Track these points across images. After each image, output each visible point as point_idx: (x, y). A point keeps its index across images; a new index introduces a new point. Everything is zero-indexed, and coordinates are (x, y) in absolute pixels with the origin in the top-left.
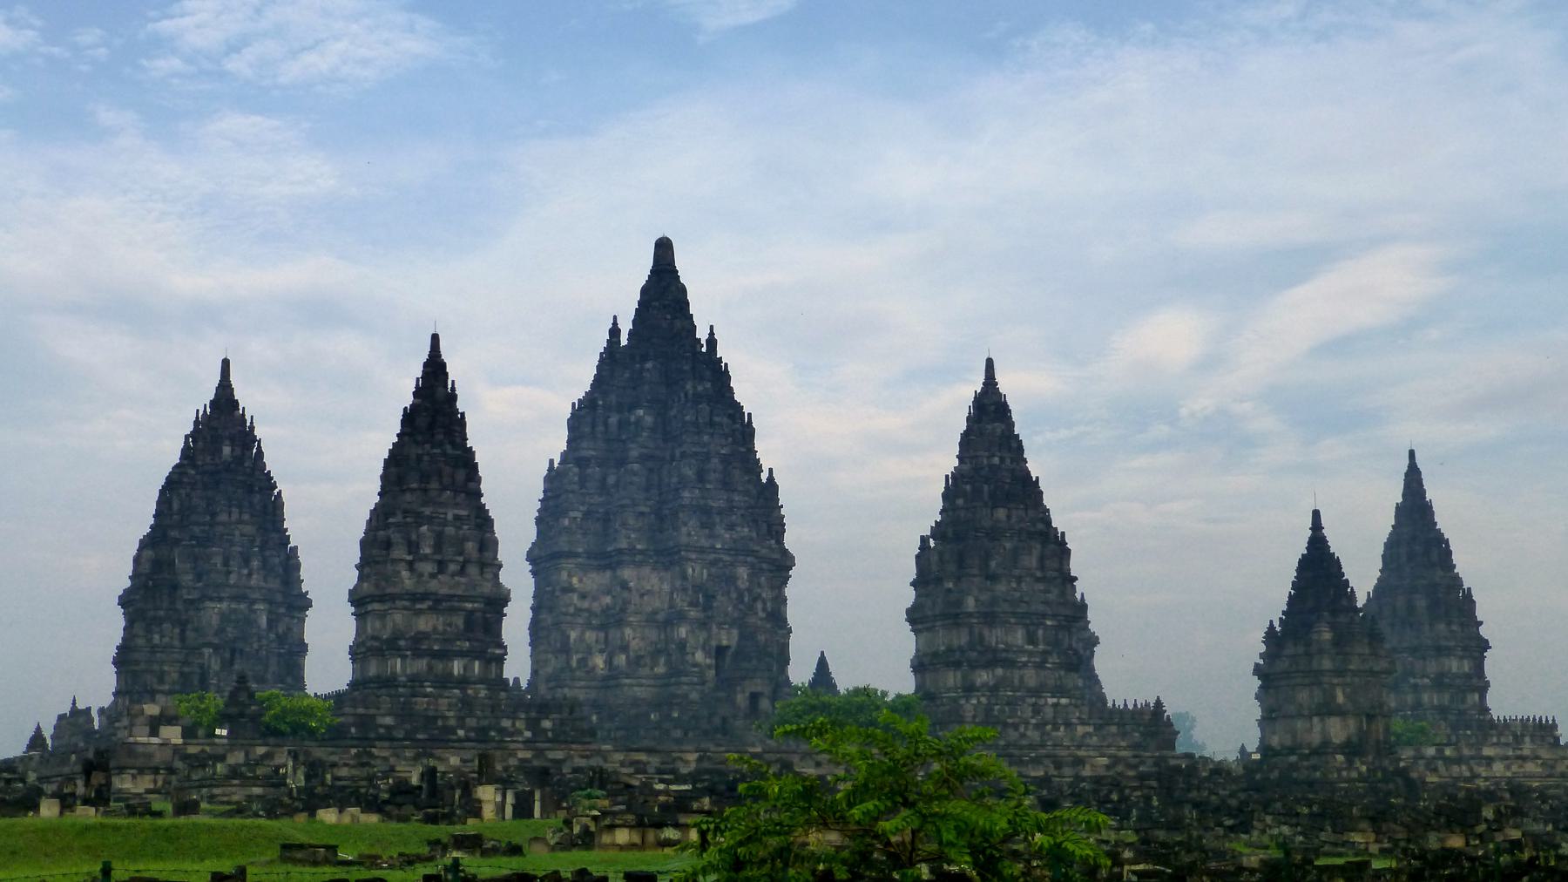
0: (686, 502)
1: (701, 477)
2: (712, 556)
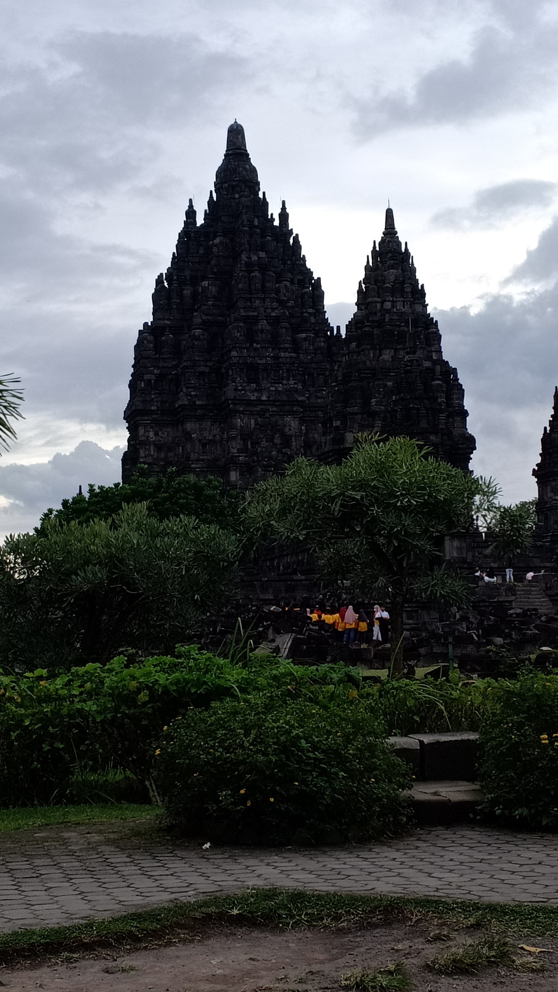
0: (235, 360)
1: (250, 337)
2: (259, 408)
